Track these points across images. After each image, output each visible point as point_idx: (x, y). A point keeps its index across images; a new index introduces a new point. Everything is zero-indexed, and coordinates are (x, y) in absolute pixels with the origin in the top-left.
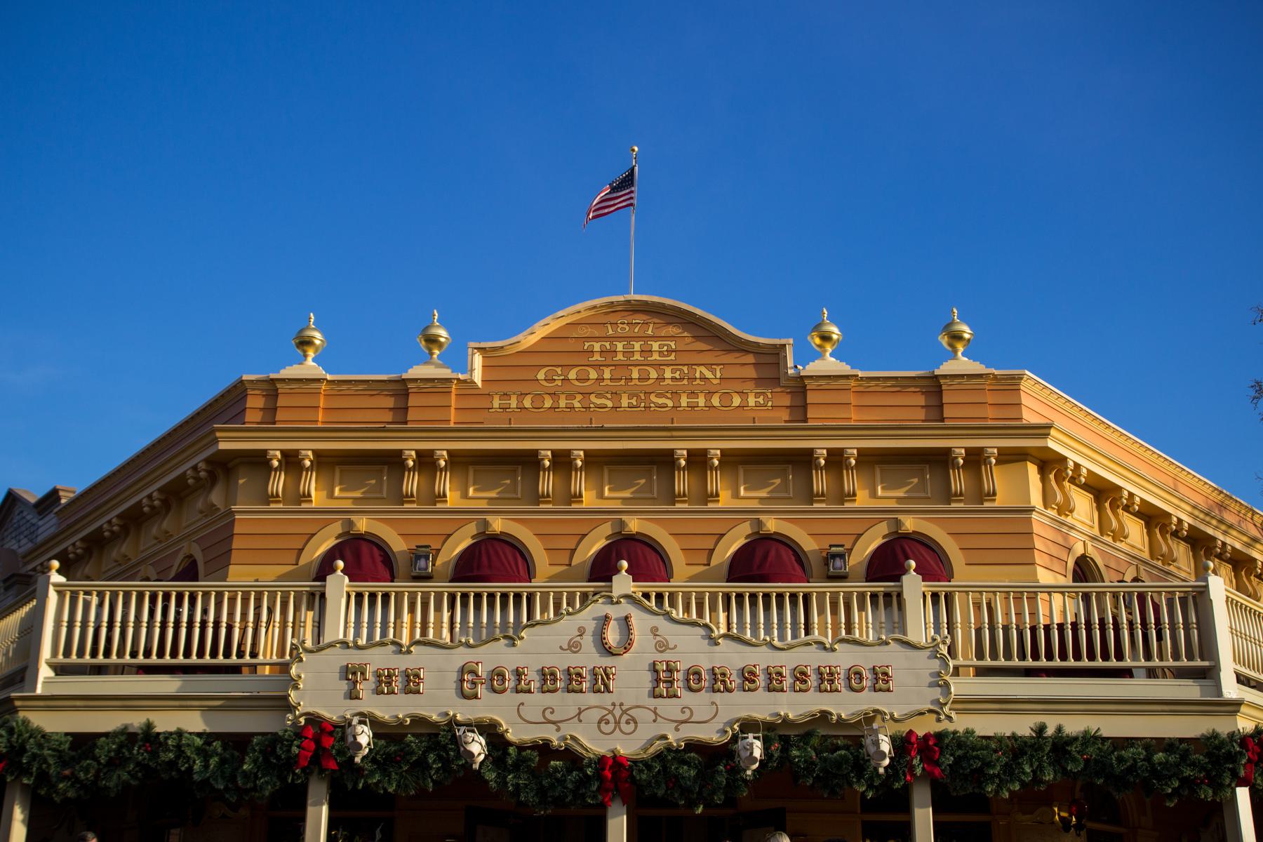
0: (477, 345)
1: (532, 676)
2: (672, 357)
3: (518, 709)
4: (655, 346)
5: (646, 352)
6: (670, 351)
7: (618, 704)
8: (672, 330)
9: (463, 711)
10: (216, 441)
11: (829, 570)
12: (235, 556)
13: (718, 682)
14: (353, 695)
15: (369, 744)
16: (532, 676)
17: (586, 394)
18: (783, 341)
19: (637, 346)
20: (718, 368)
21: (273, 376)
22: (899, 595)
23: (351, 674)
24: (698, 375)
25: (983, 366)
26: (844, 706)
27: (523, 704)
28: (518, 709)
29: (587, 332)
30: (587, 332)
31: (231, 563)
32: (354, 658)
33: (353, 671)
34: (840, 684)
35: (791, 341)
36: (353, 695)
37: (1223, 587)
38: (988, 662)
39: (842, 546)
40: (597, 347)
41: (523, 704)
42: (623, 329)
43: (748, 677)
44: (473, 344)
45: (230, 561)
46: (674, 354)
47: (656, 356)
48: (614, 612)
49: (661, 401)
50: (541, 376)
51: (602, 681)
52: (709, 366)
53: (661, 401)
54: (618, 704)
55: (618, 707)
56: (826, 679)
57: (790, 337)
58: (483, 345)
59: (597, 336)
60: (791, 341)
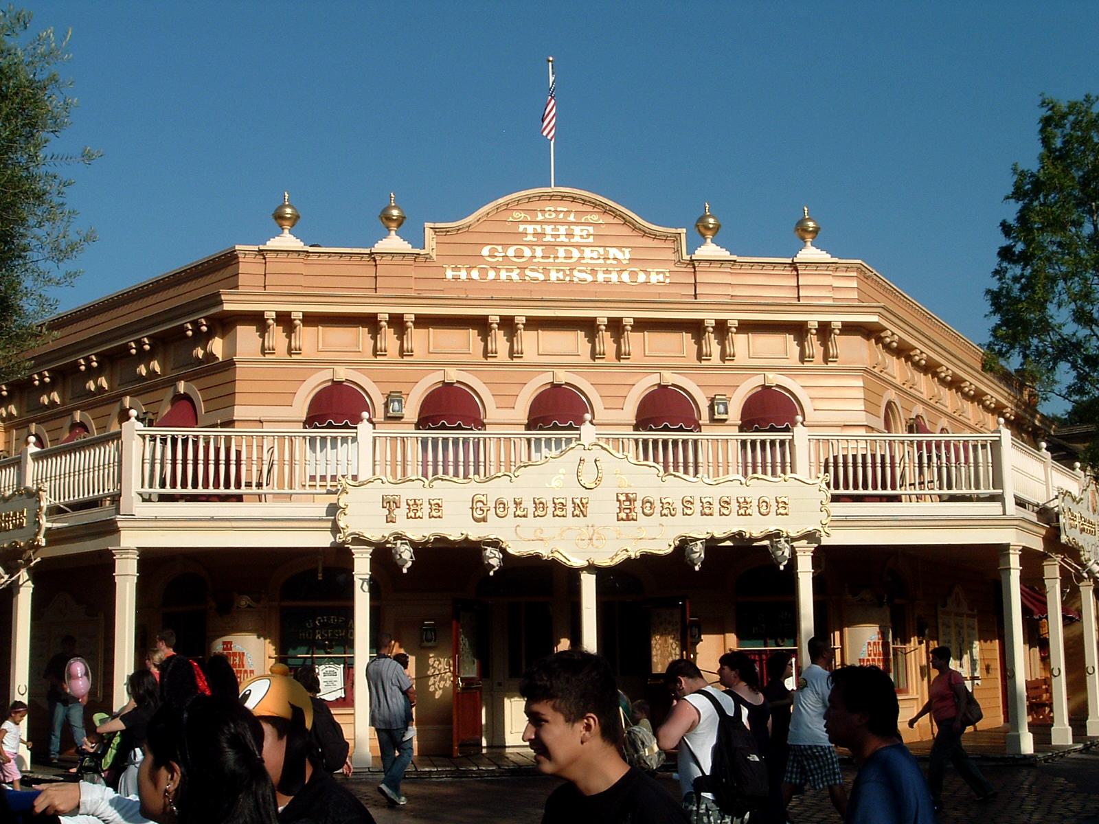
0: (432, 225)
1: (528, 505)
2: (591, 239)
3: (516, 530)
4: (577, 230)
5: (570, 235)
6: (588, 235)
7: (590, 525)
8: (594, 218)
9: (475, 533)
10: (221, 303)
11: (714, 415)
12: (238, 399)
13: (668, 511)
14: (390, 520)
15: (411, 558)
16: (528, 505)
17: (522, 269)
18: (679, 231)
19: (562, 230)
20: (627, 251)
21: (262, 247)
22: (791, 441)
23: (390, 504)
24: (611, 256)
25: (829, 256)
26: (755, 527)
27: (518, 526)
28: (516, 530)
29: (521, 217)
30: (521, 217)
31: (236, 403)
32: (391, 490)
33: (388, 501)
34: (753, 510)
35: (684, 230)
36: (390, 520)
37: (1010, 437)
38: (841, 491)
39: (725, 395)
40: (530, 229)
41: (518, 526)
42: (550, 215)
43: (687, 504)
44: (428, 225)
45: (234, 402)
46: (592, 237)
47: (577, 239)
48: (589, 457)
49: (583, 276)
50: (485, 251)
51: (581, 509)
52: (619, 247)
53: (583, 276)
54: (590, 525)
55: (590, 529)
56: (744, 505)
57: (684, 228)
58: (438, 225)
59: (529, 219)
60: (684, 230)
